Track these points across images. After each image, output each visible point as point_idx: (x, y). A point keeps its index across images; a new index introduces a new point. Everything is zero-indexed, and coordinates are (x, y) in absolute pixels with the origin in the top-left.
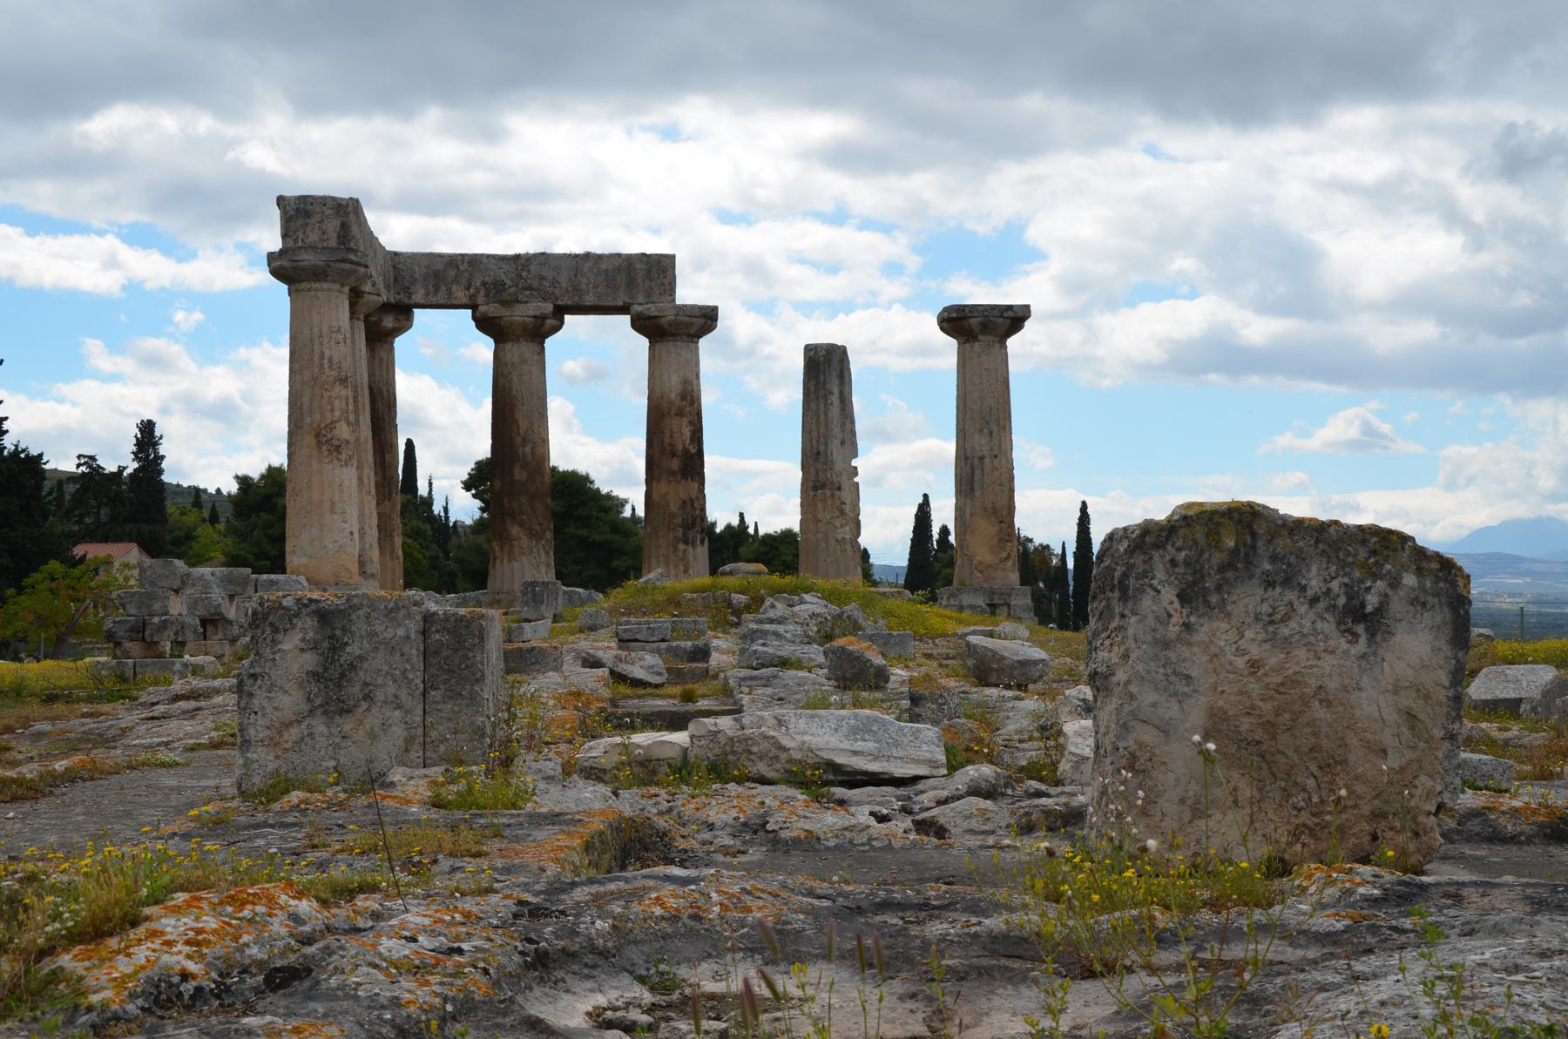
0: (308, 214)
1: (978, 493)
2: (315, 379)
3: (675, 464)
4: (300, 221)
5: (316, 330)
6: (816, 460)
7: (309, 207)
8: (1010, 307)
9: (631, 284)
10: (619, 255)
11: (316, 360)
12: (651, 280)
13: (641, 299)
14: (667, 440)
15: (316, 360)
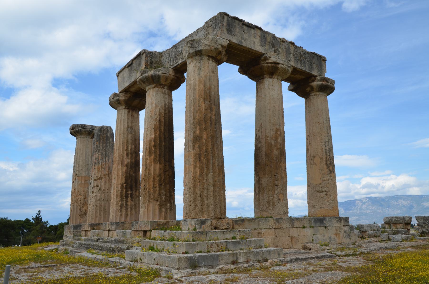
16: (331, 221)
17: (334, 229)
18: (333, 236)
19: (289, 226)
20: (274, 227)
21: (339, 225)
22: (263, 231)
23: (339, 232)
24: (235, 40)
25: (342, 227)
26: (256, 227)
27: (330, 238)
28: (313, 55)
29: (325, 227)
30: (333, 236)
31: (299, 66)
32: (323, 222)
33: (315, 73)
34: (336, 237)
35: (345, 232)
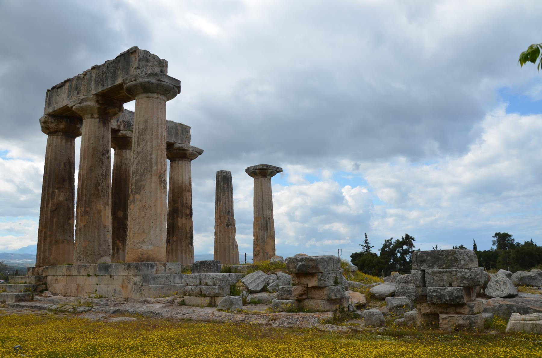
0: (147, 61)
1: (269, 230)
2: (159, 146)
3: (188, 211)
4: (144, 63)
5: (160, 120)
6: (228, 214)
7: (148, 57)
8: (278, 168)
9: (176, 134)
10: (173, 122)
11: (160, 136)
12: (183, 135)
13: (179, 142)
14: (185, 201)
15: (160, 136)
16: (118, 269)
17: (121, 278)
18: (118, 288)
19: (76, 274)
20: (66, 274)
21: (127, 274)
22: (59, 278)
23: (127, 284)
24: (50, 110)
25: (132, 277)
26: (54, 274)
27: (115, 290)
28: (119, 59)
29: (111, 277)
30: (118, 288)
31: (100, 89)
32: (108, 270)
33: (119, 81)
34: (121, 289)
35: (135, 284)
